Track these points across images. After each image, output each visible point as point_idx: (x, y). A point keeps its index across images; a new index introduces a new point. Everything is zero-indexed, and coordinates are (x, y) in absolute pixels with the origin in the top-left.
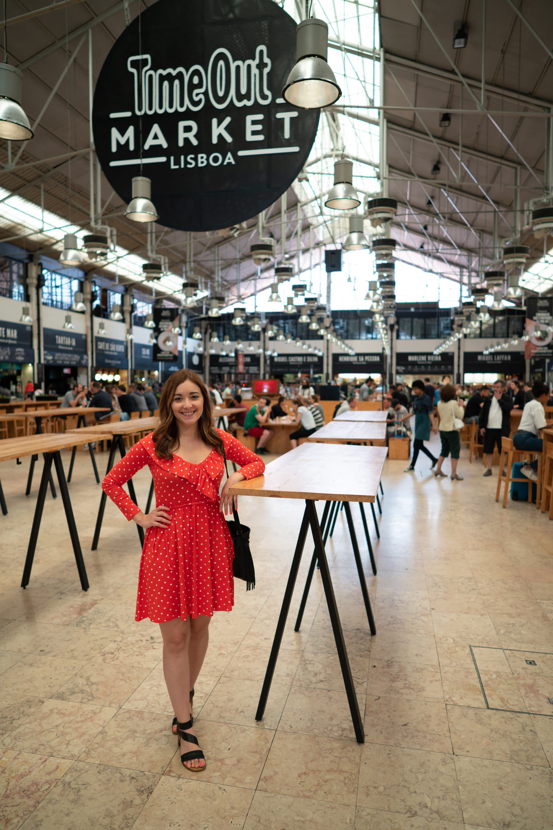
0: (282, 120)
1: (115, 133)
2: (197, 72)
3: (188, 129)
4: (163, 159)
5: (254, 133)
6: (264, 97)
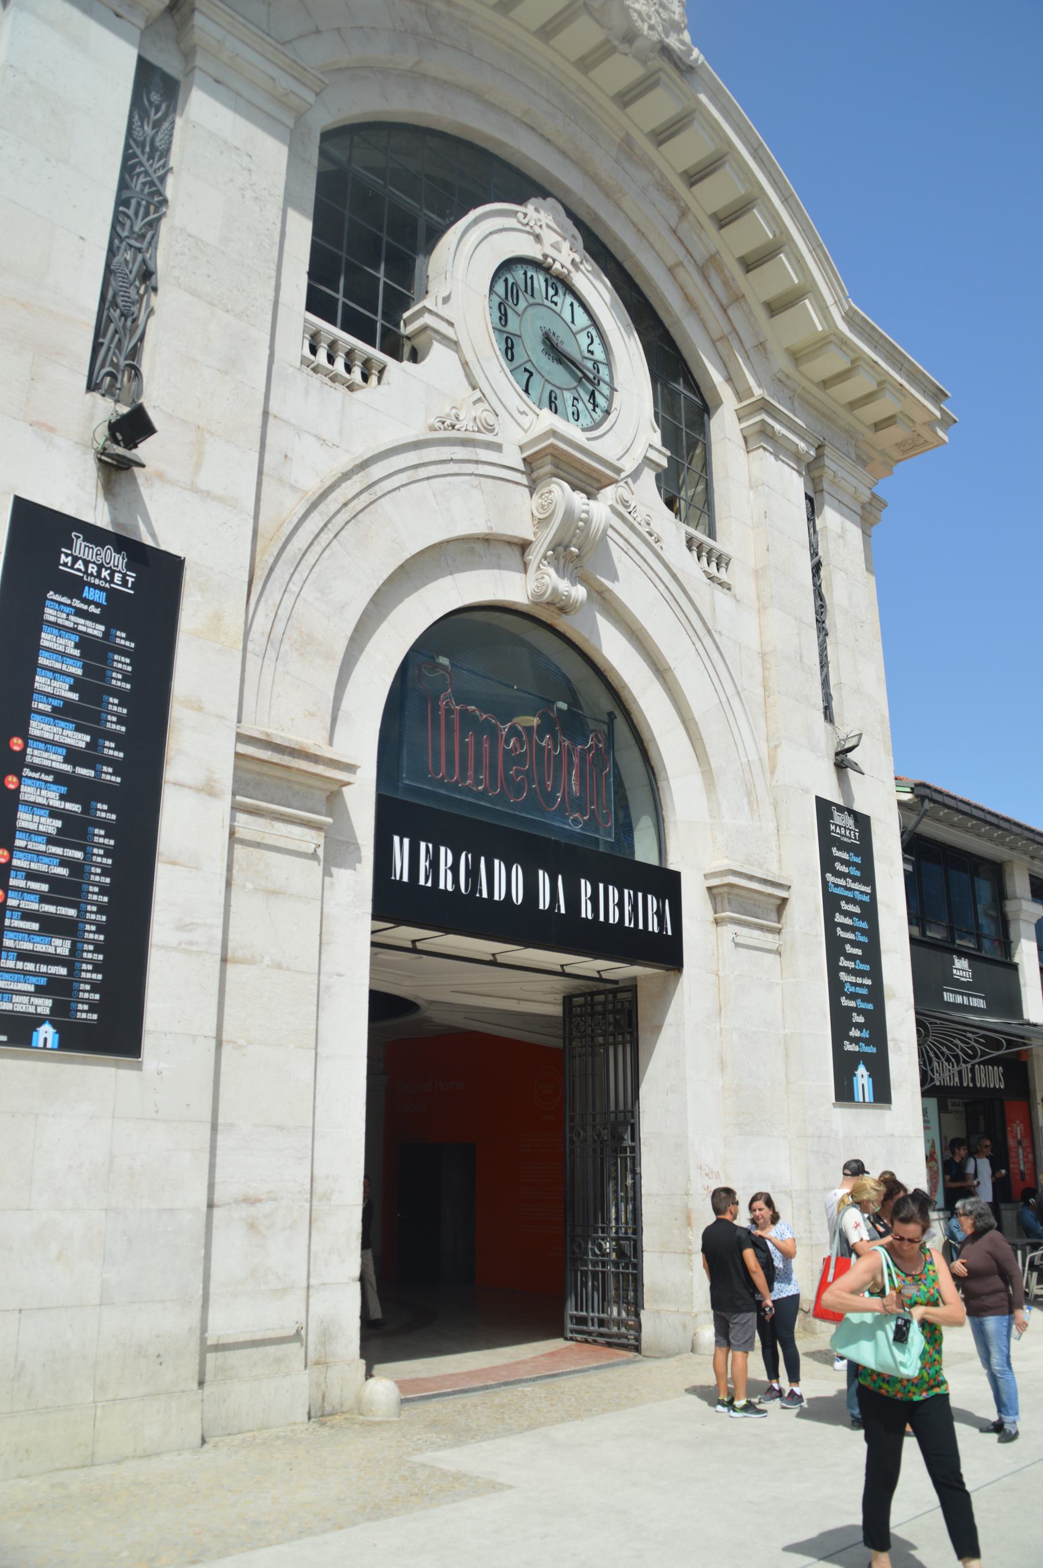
0: (128, 581)
4: (81, 575)
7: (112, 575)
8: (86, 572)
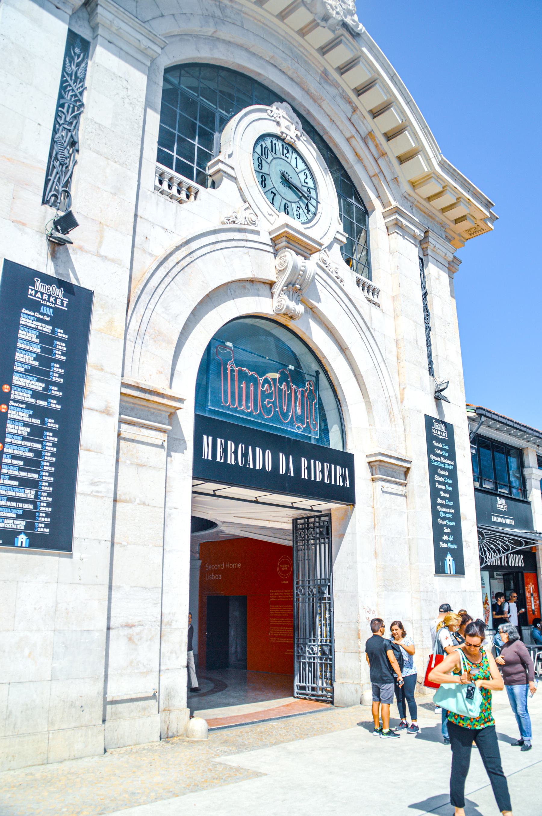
4: (40, 300)
7: (56, 300)
8: (42, 299)
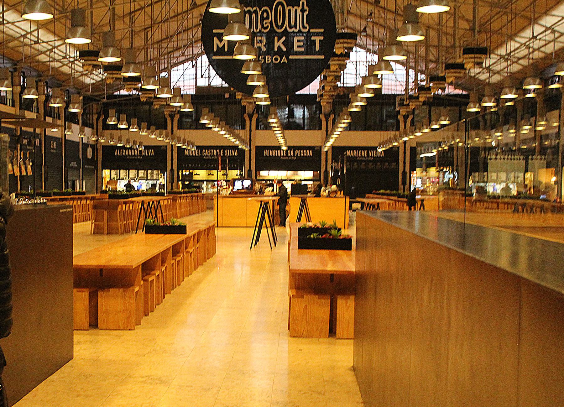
0: (314, 42)
1: (216, 40)
2: (266, 11)
3: (261, 41)
5: (298, 47)
6: (305, 28)
7: (289, 44)
